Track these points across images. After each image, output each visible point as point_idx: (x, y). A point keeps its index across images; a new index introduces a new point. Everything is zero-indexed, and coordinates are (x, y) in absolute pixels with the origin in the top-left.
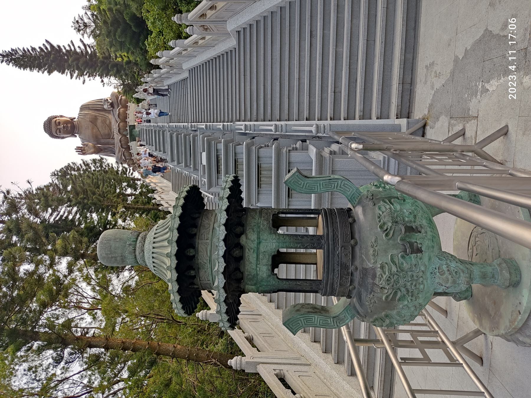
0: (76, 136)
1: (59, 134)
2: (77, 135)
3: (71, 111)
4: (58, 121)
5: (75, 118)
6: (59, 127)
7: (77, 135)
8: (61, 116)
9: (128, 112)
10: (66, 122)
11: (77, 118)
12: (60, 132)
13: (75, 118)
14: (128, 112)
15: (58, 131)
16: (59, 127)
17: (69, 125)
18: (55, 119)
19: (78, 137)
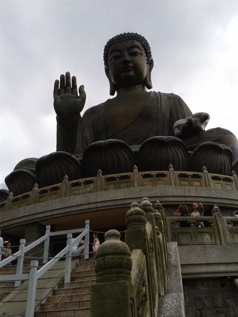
0: (112, 93)
1: (112, 56)
4: (138, 51)
5: (150, 87)
6: (126, 53)
8: (151, 64)
9: (172, 173)
10: (137, 69)
11: (152, 90)
12: (116, 58)
13: (150, 87)
14: (172, 173)
15: (117, 54)
16: (126, 53)
17: (132, 73)
18: (142, 49)
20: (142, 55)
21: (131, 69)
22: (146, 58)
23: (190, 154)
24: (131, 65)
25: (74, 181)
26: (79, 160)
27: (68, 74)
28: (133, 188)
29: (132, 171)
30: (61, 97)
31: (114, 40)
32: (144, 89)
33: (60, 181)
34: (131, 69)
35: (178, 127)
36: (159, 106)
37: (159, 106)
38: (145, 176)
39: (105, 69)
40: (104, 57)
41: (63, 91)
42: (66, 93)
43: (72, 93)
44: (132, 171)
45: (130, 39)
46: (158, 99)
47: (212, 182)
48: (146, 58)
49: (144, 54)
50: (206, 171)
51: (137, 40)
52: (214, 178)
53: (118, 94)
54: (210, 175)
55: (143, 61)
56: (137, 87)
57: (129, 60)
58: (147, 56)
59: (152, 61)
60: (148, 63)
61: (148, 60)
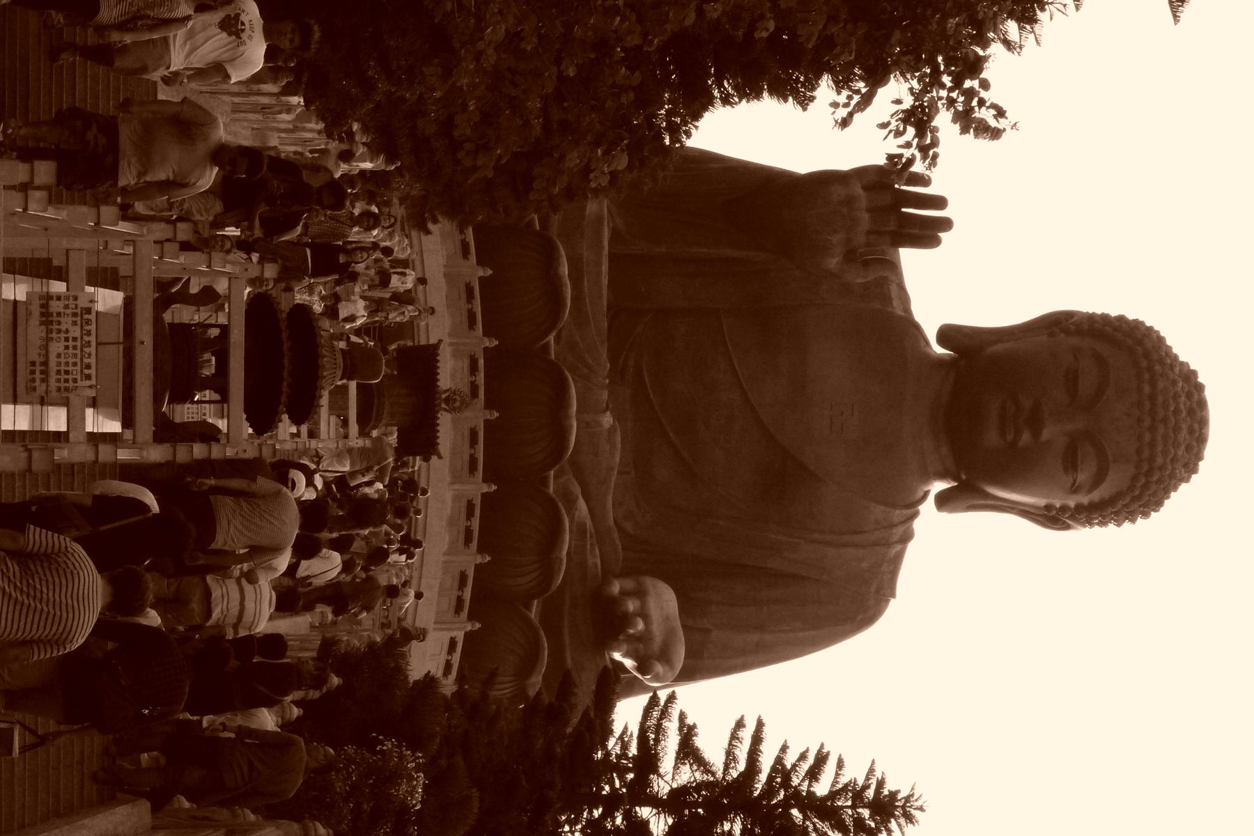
2: (939, 350)
3: (964, 560)
4: (1083, 477)
7: (939, 350)
8: (1052, 518)
9: (471, 560)
11: (928, 508)
12: (1072, 378)
13: (943, 501)
14: (471, 560)
17: (992, 438)
19: (931, 334)
20: (1075, 490)
21: (1010, 437)
22: (1072, 504)
23: (528, 606)
24: (1026, 438)
25: (481, 362)
26: (548, 344)
27: (946, 224)
28: (448, 479)
29: (484, 481)
30: (850, 201)
31: (1153, 384)
32: (942, 476)
33: (487, 333)
34: (1010, 437)
35: (640, 593)
36: (816, 536)
37: (816, 536)
38: (470, 506)
39: (1069, 315)
40: (1121, 319)
41: (887, 199)
42: (869, 210)
43: (869, 233)
44: (484, 481)
45: (1139, 452)
46: (856, 533)
47: (445, 637)
48: (1072, 504)
49: (1085, 499)
50: (469, 628)
51: (1135, 479)
52: (453, 643)
53: (940, 362)
54: (460, 636)
55: (1179, 470)
56: (944, 450)
57: (1046, 434)
58: (1079, 508)
59: (1067, 527)
60: (1048, 507)
61: (1064, 509)
